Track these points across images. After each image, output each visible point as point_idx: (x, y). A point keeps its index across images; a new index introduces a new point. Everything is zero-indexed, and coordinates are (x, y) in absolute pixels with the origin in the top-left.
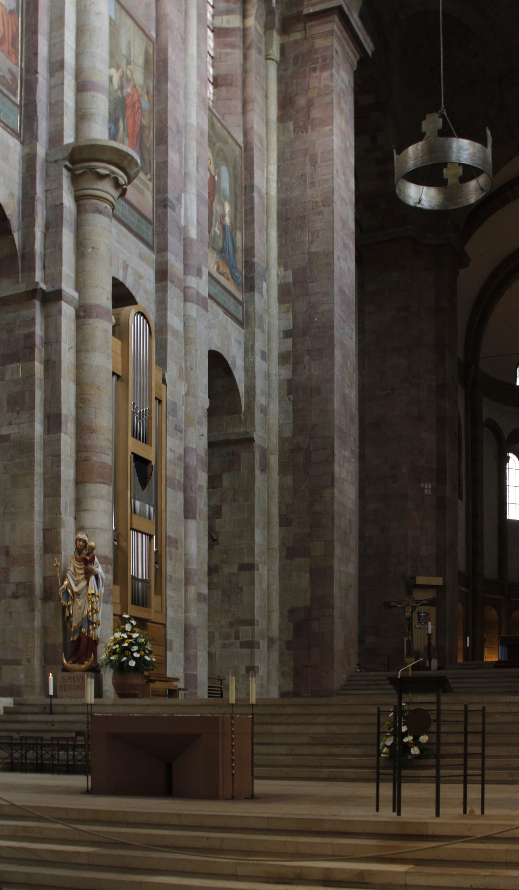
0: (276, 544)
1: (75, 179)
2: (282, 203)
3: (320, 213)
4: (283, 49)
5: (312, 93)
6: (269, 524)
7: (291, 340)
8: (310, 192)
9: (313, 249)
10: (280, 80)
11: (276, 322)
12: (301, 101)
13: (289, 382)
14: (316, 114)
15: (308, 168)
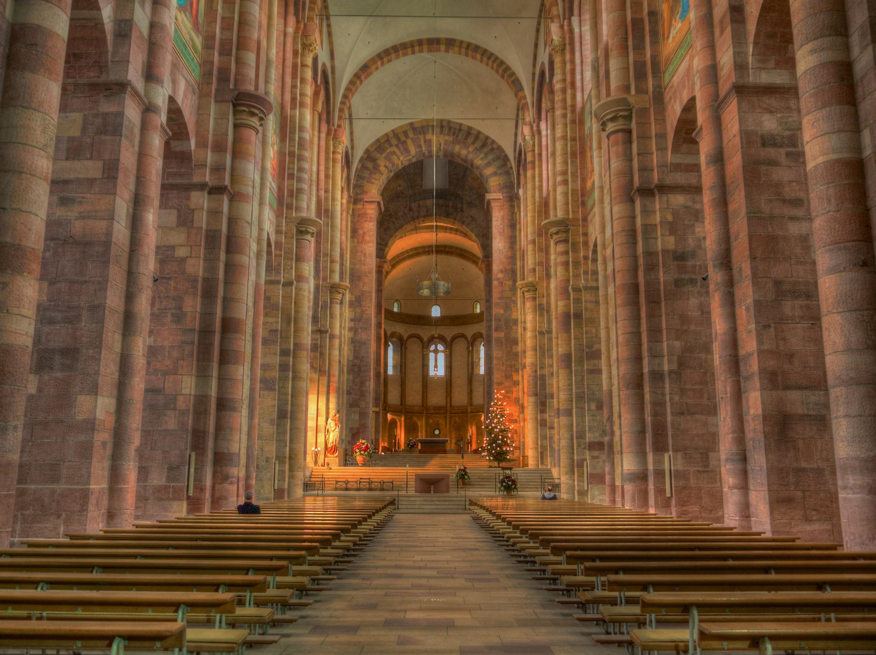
0: (345, 402)
1: (331, 292)
2: (352, 269)
3: (367, 276)
4: (353, 210)
5: (365, 230)
6: (343, 393)
7: (353, 323)
8: (363, 267)
9: (364, 289)
10: (352, 222)
11: (347, 315)
12: (361, 232)
13: (352, 338)
14: (367, 238)
15: (363, 258)
